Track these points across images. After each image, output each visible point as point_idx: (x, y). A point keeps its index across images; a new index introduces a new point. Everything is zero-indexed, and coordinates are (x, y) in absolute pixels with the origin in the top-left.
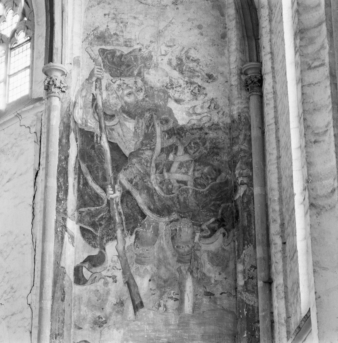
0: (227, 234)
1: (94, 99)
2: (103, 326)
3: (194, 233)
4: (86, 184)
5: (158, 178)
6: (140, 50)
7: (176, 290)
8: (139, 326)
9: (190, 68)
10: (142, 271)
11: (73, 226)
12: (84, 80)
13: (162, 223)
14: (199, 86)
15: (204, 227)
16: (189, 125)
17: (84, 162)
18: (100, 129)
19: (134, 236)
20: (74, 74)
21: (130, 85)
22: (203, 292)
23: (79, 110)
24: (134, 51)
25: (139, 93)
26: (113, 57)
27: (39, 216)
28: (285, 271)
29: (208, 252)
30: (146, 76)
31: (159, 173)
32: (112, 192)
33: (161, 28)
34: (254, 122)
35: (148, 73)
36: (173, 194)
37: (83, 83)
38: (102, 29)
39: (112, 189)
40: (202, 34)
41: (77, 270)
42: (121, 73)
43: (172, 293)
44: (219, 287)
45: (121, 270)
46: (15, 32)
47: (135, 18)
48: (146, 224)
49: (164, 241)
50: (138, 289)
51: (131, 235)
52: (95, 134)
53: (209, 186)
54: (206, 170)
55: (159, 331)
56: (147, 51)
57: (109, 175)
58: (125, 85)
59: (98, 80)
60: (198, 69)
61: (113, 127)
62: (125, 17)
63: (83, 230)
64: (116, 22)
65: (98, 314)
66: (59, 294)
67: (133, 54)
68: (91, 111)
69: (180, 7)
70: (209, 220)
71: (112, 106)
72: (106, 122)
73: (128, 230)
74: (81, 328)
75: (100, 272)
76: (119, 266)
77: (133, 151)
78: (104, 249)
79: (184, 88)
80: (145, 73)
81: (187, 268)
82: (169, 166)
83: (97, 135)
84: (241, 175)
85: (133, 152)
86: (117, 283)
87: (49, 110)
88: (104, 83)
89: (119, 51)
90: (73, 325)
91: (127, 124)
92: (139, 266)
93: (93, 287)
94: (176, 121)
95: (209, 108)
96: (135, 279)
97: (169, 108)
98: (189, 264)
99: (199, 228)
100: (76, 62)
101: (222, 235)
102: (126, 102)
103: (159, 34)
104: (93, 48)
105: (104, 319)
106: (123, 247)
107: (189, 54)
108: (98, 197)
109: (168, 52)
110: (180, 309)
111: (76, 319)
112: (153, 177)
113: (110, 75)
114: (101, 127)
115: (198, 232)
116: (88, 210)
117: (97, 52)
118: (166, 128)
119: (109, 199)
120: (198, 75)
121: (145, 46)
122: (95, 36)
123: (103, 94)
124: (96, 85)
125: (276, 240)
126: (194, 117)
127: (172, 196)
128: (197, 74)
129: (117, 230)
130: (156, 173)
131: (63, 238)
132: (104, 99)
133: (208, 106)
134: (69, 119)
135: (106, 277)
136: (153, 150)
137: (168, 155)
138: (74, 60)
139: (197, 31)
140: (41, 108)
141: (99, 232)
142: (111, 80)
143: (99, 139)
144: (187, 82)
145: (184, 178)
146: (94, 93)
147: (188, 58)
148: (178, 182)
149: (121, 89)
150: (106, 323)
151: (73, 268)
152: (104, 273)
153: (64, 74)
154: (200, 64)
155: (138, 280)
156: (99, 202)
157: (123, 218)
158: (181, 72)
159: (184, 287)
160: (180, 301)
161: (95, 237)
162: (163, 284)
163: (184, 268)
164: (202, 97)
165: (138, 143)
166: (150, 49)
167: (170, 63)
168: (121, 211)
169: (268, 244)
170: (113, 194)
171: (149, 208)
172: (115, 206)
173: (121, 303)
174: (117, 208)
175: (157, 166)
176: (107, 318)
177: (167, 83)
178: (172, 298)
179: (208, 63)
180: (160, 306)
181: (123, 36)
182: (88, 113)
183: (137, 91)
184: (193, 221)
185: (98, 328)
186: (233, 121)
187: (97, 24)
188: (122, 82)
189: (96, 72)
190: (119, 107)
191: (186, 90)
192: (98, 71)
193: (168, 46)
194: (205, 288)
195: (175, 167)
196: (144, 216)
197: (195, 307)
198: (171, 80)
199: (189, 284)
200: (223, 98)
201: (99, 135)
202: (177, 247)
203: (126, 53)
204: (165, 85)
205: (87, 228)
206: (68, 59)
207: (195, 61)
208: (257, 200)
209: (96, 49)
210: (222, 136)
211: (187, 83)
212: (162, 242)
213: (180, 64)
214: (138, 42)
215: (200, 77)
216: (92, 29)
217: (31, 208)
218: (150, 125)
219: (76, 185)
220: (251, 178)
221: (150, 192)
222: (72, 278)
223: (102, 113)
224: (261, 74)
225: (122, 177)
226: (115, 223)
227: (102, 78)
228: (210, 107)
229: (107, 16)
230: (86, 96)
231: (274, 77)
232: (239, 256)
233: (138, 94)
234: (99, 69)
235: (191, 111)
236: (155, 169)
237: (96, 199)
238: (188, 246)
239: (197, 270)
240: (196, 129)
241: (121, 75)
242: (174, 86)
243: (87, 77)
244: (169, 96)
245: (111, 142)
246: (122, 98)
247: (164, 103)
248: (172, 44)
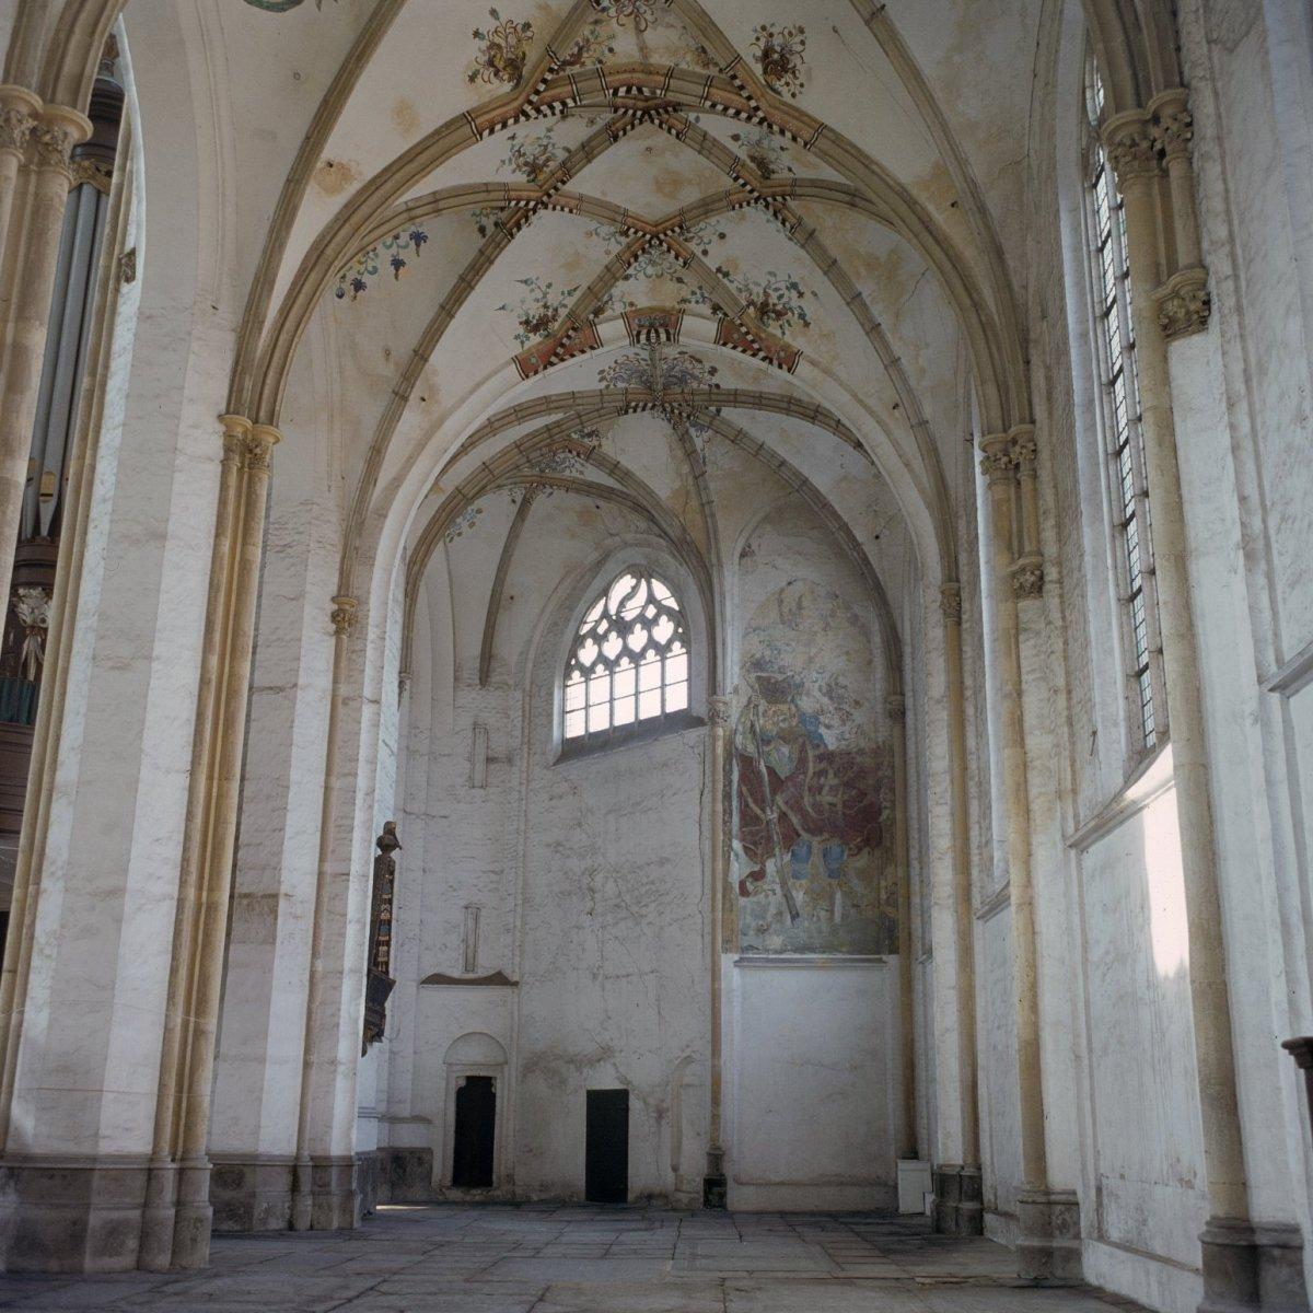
1: (752, 726)
3: (843, 851)
4: (747, 806)
11: (736, 845)
15: (852, 846)
20: (734, 702)
26: (769, 683)
27: (707, 834)
28: (921, 893)
33: (812, 654)
34: (897, 750)
38: (758, 656)
40: (849, 661)
41: (742, 884)
46: (670, 642)
47: (788, 645)
49: (816, 858)
54: (854, 792)
55: (812, 938)
59: (756, 706)
62: (778, 644)
63: (745, 848)
65: (760, 923)
66: (727, 906)
68: (750, 736)
69: (830, 634)
87: (714, 738)
88: (761, 709)
93: (755, 899)
100: (736, 690)
102: (781, 728)
103: (811, 660)
108: (758, 818)
110: (831, 919)
114: (759, 752)
118: (817, 753)
125: (915, 864)
131: (729, 857)
134: (730, 746)
136: (805, 773)
137: (819, 779)
139: (844, 657)
140: (703, 731)
145: (834, 800)
148: (830, 804)
153: (725, 703)
155: (794, 893)
158: (831, 698)
160: (831, 911)
161: (756, 854)
163: (834, 882)
164: (850, 723)
166: (802, 676)
167: (820, 690)
169: (908, 865)
171: (804, 829)
173: (780, 913)
176: (769, 926)
182: (747, 739)
186: (879, 747)
187: (753, 652)
190: (775, 733)
195: (826, 788)
196: (799, 835)
197: (844, 917)
198: (821, 707)
199: (838, 896)
206: (729, 689)
208: (899, 824)
209: (753, 676)
210: (868, 761)
211: (836, 709)
217: (697, 825)
218: (803, 750)
220: (893, 802)
221: (801, 811)
222: (738, 890)
224: (903, 705)
225: (779, 799)
231: (915, 714)
232: (882, 874)
241: (776, 702)
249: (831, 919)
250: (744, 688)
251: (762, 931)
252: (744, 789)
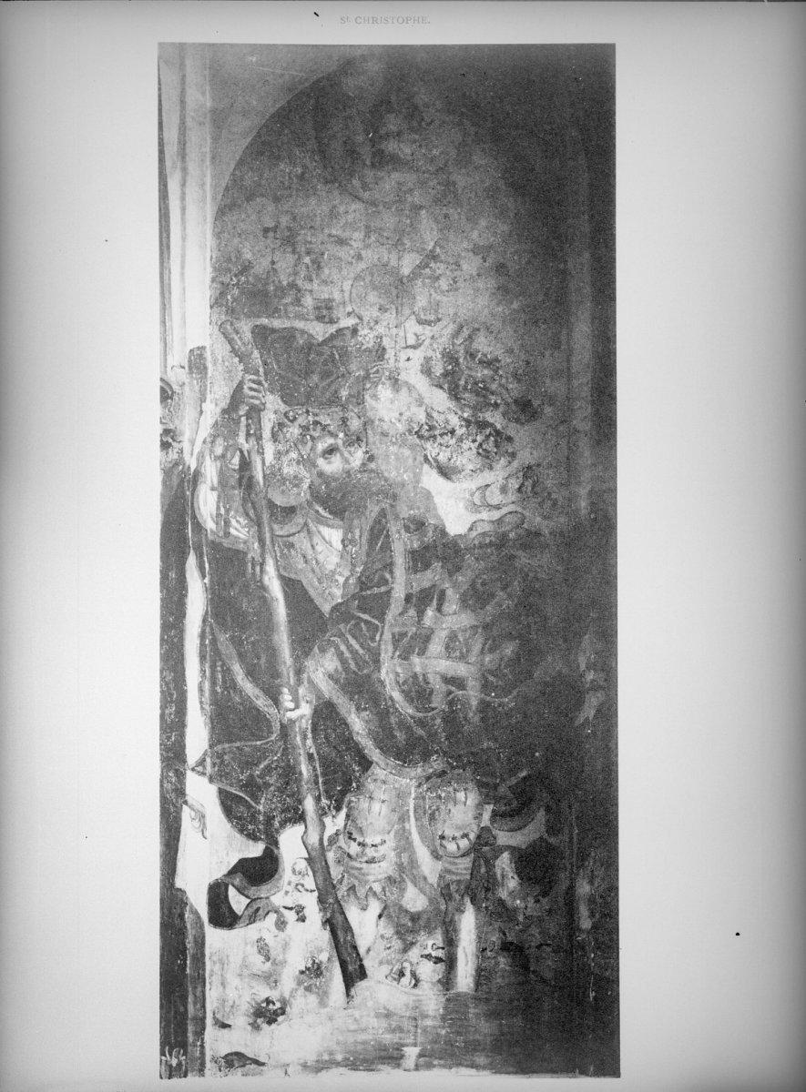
1: (245, 464)
2: (276, 1020)
4: (231, 685)
6: (355, 331)
7: (438, 938)
8: (355, 1020)
11: (202, 792)
12: (218, 410)
14: (498, 433)
16: (474, 534)
17: (223, 625)
21: (332, 428)
22: (498, 943)
23: (209, 491)
25: (352, 449)
29: (512, 849)
31: (399, 656)
32: (292, 705)
35: (375, 397)
36: (433, 709)
37: (216, 422)
41: (217, 894)
42: (308, 396)
43: (431, 942)
44: (535, 931)
45: (316, 894)
50: (353, 936)
51: (338, 809)
52: (249, 556)
56: (371, 336)
57: (285, 663)
58: (319, 427)
59: (255, 412)
60: (494, 387)
64: (294, 252)
65: (264, 992)
67: (338, 343)
68: (237, 494)
72: (276, 527)
73: (329, 798)
74: (230, 1026)
75: (267, 898)
76: (310, 882)
77: (340, 601)
78: (276, 843)
79: (461, 440)
80: (367, 397)
82: (425, 639)
85: (341, 604)
86: (307, 921)
89: (303, 332)
90: (209, 1021)
91: (325, 531)
95: (519, 490)
96: (346, 912)
102: (321, 474)
104: (237, 325)
105: (278, 1005)
106: (318, 837)
107: (475, 346)
109: (423, 338)
111: (215, 1005)
113: (282, 398)
114: (262, 541)
117: (248, 336)
119: (285, 721)
120: (496, 403)
121: (366, 319)
122: (242, 293)
123: (265, 451)
124: (248, 426)
126: (485, 515)
128: (493, 399)
129: (304, 798)
132: (267, 464)
133: (517, 486)
137: (421, 613)
138: (190, 357)
141: (263, 801)
143: (258, 569)
144: (466, 420)
145: (461, 670)
146: (246, 447)
147: (473, 356)
149: (308, 437)
150: (283, 1013)
151: (207, 889)
155: (353, 913)
156: (260, 729)
158: (455, 394)
159: (456, 931)
160: (450, 962)
162: (410, 924)
164: (503, 461)
165: (351, 581)
166: (380, 329)
167: (427, 370)
168: (313, 750)
170: (294, 710)
172: (298, 739)
173: (315, 970)
174: (304, 745)
175: (397, 640)
176: (284, 1003)
177: (421, 422)
178: (428, 957)
179: (520, 371)
180: (403, 975)
183: (349, 445)
184: (478, 775)
185: (265, 1026)
188: (311, 418)
189: (246, 390)
191: (467, 444)
192: (251, 389)
194: (505, 934)
196: (366, 764)
197: (482, 975)
198: (429, 416)
199: (468, 922)
201: (258, 558)
203: (321, 339)
204: (416, 429)
205: (234, 792)
209: (245, 327)
211: (468, 422)
213: (453, 373)
214: (349, 309)
215: (501, 409)
216: (235, 270)
218: (378, 533)
219: (207, 685)
223: (264, 502)
226: (298, 781)
228: (524, 489)
229: (271, 234)
230: (223, 456)
233: (350, 452)
234: (254, 382)
235: (478, 502)
236: (390, 648)
237: (254, 722)
239: (486, 891)
242: (437, 432)
243: (224, 404)
244: (426, 459)
246: (314, 465)
248: (432, 318)
249: (447, 982)
250: (217, 350)
251: (267, 1014)
252: (223, 638)
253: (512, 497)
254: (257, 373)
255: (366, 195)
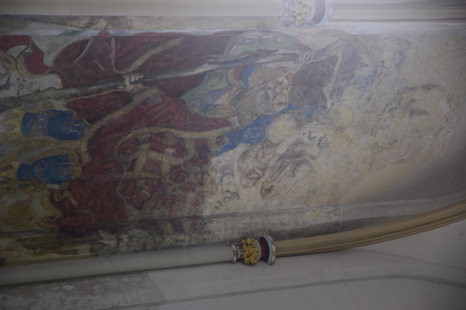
0: (54, 220)
5: (144, 136)
9: (286, 166)
10: (13, 122)
13: (79, 144)
15: (67, 194)
18: (226, 61)
19: (64, 109)
24: (325, 101)
30: (287, 116)
32: (133, 80)
36: (119, 155)
39: (137, 79)
45: (16, 96)
47: (368, 99)
48: (80, 124)
51: (67, 106)
53: (122, 197)
59: (294, 58)
61: (225, 78)
70: (75, 199)
71: (255, 75)
75: (16, 68)
76: (24, 92)
78: (50, 73)
81: (11, 176)
83: (218, 58)
84: (131, 238)
92: (21, 118)
94: (218, 154)
95: (228, 191)
97: (238, 145)
98: (16, 179)
99: (66, 188)
101: (52, 214)
103: (340, 129)
109: (313, 141)
112: (146, 130)
114: (227, 62)
115: (60, 187)
116: (112, 50)
117: (333, 54)
127: (116, 154)
130: (151, 133)
133: (230, 190)
135: (8, 77)
142: (290, 74)
143: (212, 60)
145: (139, 168)
148: (135, 160)
152: (14, 75)
154: (288, 178)
157: (94, 96)
163: (11, 174)
167: (297, 143)
171: (102, 127)
181: (348, 85)
192: (307, 56)
193: (320, 140)
196: (92, 122)
200: (237, 206)
202: (43, 163)
207: (293, 172)
212: (53, 144)
227: (296, 62)
234: (311, 56)
238: (42, 176)
240: (202, 178)
245: (205, 76)
247: (245, 138)
253: (225, 188)
254: (315, 58)
255: (388, 109)
